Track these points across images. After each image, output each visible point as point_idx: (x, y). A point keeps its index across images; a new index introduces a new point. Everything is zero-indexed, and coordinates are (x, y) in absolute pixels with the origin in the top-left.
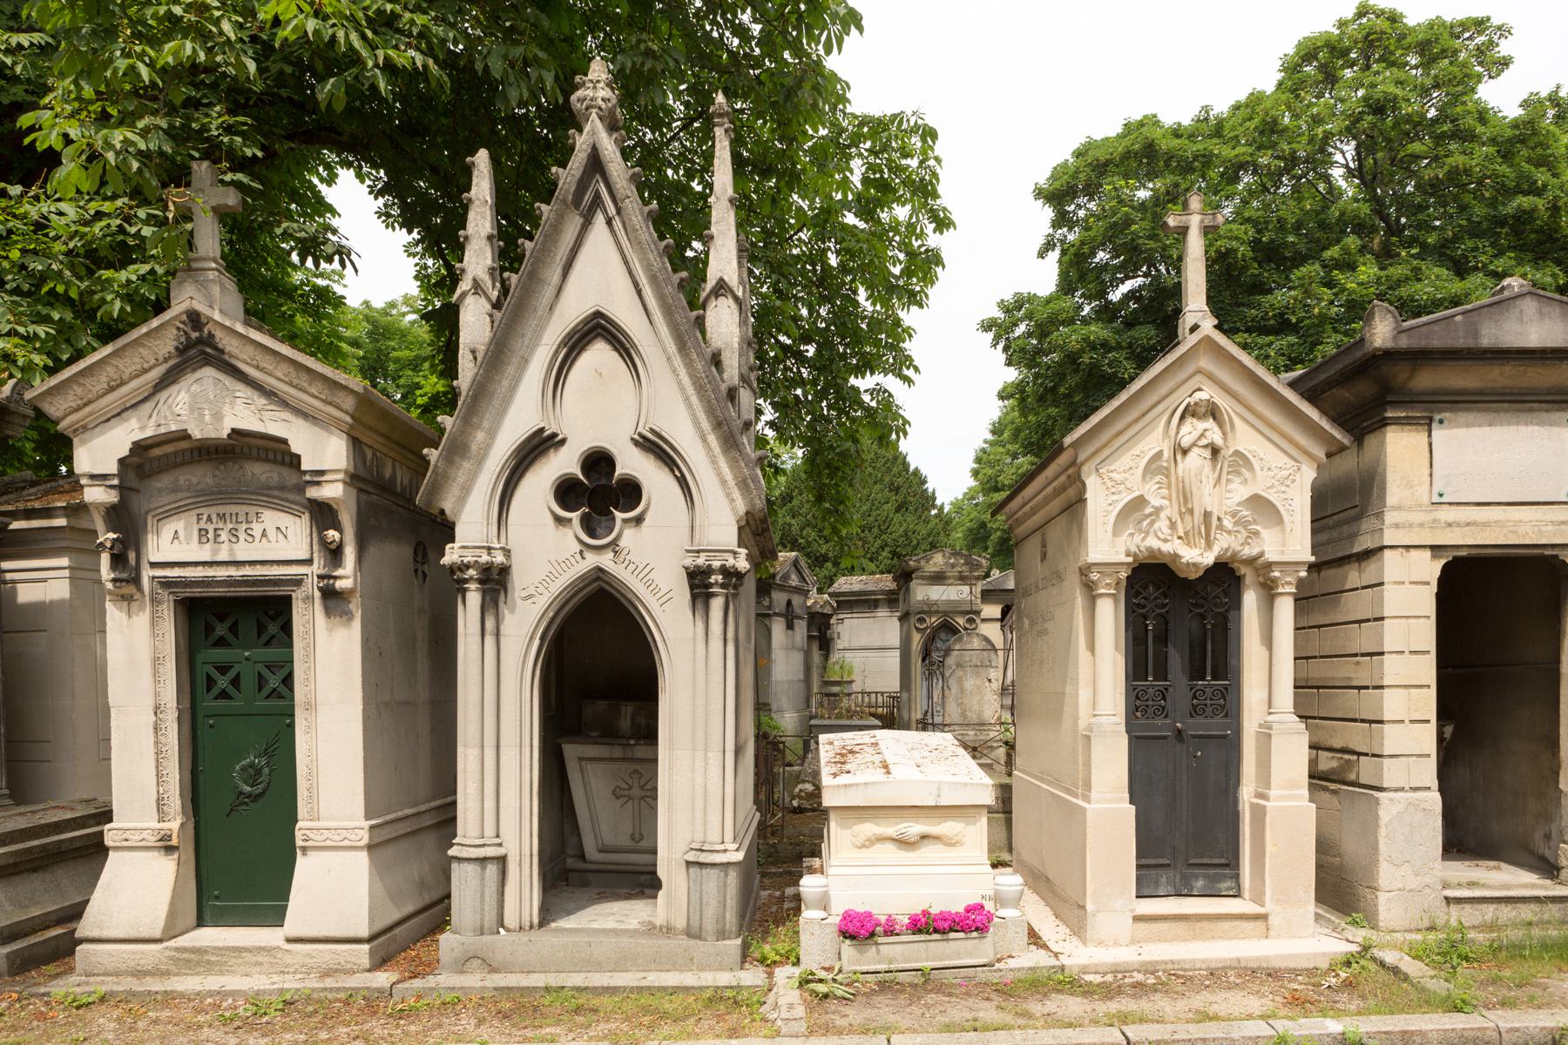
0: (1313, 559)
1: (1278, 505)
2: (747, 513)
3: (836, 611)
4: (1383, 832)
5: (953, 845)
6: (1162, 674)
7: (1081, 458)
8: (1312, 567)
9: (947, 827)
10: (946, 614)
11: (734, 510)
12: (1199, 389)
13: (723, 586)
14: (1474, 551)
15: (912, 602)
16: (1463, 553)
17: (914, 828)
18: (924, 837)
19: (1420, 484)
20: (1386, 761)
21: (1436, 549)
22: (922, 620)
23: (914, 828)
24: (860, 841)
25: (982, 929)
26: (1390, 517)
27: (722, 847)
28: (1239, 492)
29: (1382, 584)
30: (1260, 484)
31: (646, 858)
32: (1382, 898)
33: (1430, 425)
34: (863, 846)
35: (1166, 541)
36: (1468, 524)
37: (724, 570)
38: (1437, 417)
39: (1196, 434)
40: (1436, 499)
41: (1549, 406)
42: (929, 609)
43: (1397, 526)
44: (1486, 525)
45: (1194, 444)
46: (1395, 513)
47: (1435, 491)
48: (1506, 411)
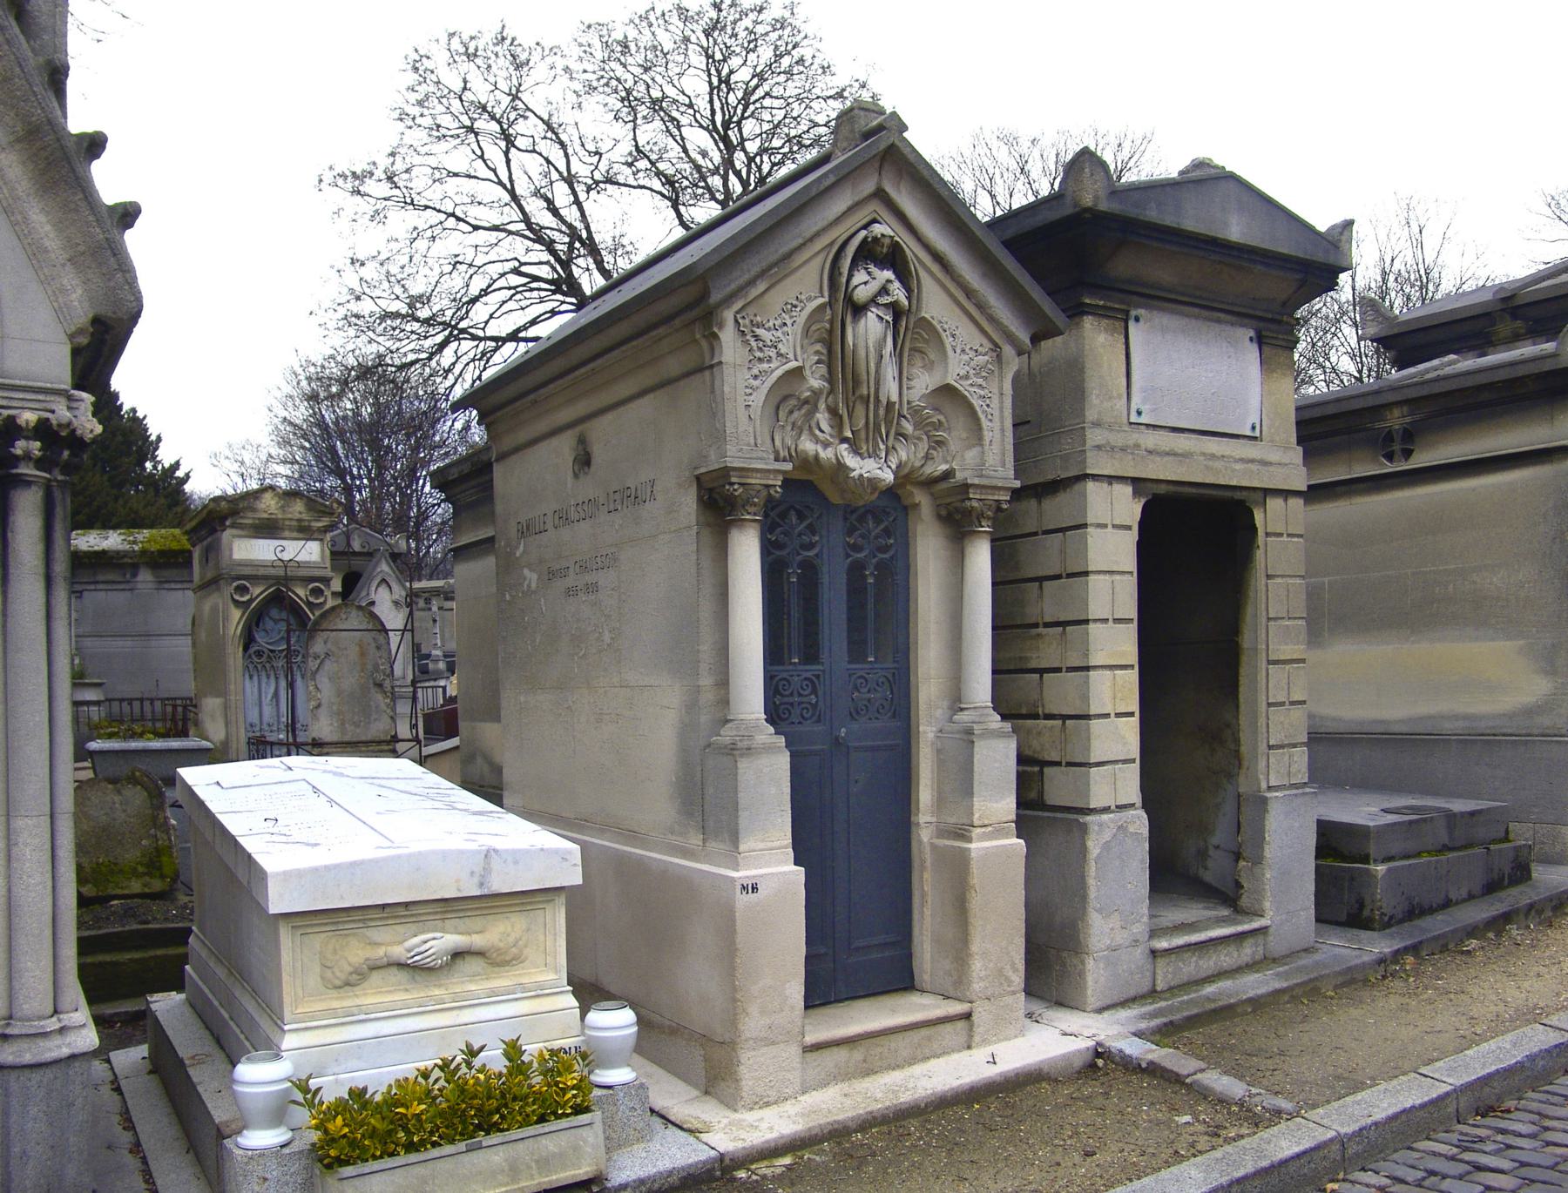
0: (1017, 484)
1: (976, 403)
2: (97, 321)
3: (291, 529)
4: (1092, 870)
5: (507, 963)
6: (811, 654)
7: (715, 297)
8: (1017, 494)
9: (494, 932)
10: (278, 580)
11: (60, 313)
12: (874, 221)
13: (40, 464)
14: (1172, 488)
15: (224, 562)
16: (1162, 489)
17: (439, 941)
18: (458, 955)
19: (1120, 396)
20: (1093, 770)
21: (1137, 483)
22: (242, 590)
23: (439, 941)
24: (342, 972)
25: (1033, 989)
26: (1094, 437)
27: (52, 1024)
28: (923, 383)
29: (1085, 526)
30: (955, 369)
31: (109, 1009)
32: (1090, 964)
33: (1126, 322)
34: (348, 984)
35: (826, 445)
36: (1168, 454)
37: (43, 430)
38: (1133, 313)
39: (874, 287)
40: (1134, 419)
41: (1234, 319)
42: (248, 575)
43: (1099, 447)
44: (1186, 455)
45: (873, 301)
46: (1097, 431)
47: (1134, 407)
48: (1197, 317)
